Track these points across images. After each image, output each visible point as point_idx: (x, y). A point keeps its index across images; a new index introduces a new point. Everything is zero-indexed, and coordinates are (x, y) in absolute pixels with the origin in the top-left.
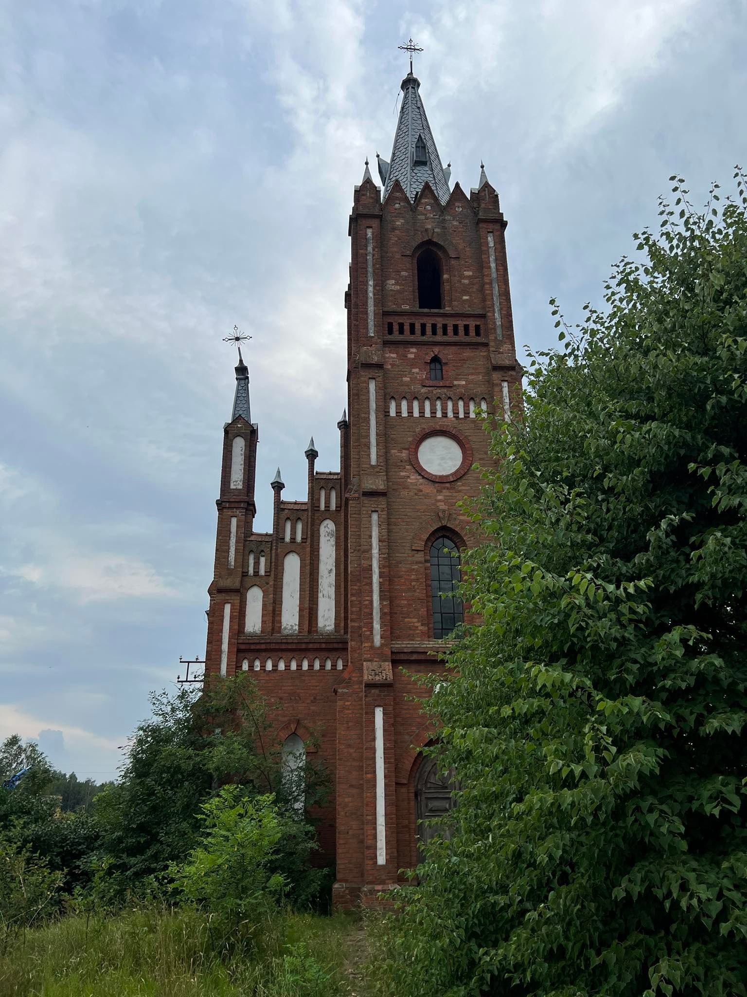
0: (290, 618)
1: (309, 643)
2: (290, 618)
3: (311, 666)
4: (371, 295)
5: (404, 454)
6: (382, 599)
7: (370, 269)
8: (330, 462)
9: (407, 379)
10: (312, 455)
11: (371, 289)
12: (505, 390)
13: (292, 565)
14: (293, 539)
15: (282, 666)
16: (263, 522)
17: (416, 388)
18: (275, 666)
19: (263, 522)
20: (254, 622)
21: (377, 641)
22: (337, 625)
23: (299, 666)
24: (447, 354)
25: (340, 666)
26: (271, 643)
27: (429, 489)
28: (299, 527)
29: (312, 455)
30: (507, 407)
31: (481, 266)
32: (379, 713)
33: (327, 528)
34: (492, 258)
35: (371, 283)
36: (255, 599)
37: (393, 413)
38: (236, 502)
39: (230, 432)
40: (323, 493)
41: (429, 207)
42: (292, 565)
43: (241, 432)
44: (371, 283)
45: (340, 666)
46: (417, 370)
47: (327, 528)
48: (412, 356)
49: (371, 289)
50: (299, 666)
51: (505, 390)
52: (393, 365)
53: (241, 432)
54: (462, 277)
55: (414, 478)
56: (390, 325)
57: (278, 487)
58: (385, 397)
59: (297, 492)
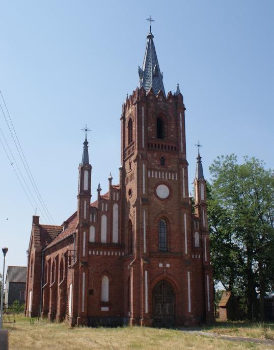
0: (104, 239)
1: (109, 245)
2: (104, 239)
3: (111, 254)
5: (152, 191)
6: (146, 239)
7: (143, 122)
8: (116, 182)
9: (153, 164)
10: (110, 180)
12: (183, 171)
13: (104, 219)
14: (104, 210)
15: (101, 253)
18: (99, 253)
20: (92, 238)
21: (145, 251)
22: (119, 241)
23: (107, 254)
24: (166, 155)
25: (123, 254)
26: (97, 245)
27: (160, 203)
28: (106, 205)
29: (110, 180)
30: (184, 177)
33: (116, 207)
34: (181, 122)
36: (92, 230)
37: (149, 176)
38: (84, 195)
40: (114, 193)
41: (161, 99)
42: (104, 219)
43: (86, 168)
45: (123, 254)
46: (156, 161)
48: (155, 156)
50: (107, 254)
51: (183, 171)
52: (150, 159)
53: (86, 168)
54: (171, 128)
55: (155, 199)
56: (149, 144)
57: (99, 190)
58: (148, 169)
59: (105, 191)
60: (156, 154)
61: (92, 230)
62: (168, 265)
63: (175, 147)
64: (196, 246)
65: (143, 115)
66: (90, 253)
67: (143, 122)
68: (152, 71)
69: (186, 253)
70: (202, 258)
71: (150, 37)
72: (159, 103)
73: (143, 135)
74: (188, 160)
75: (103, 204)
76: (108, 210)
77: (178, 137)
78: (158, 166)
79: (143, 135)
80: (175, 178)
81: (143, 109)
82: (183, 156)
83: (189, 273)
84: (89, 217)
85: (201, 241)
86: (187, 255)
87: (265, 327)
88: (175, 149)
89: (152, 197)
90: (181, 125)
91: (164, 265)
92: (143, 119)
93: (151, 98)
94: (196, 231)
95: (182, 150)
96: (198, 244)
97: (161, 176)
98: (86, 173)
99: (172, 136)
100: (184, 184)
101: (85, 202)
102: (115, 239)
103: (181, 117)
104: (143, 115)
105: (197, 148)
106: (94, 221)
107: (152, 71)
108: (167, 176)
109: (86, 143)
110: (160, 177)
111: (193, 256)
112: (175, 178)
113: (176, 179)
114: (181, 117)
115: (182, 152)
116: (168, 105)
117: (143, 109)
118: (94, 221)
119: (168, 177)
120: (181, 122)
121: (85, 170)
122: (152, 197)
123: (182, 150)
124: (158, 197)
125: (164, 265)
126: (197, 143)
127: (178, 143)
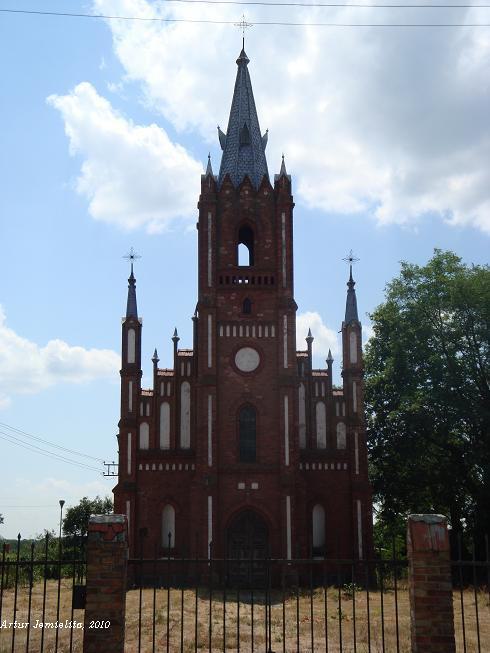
0: (165, 442)
2: (165, 442)
4: (210, 259)
5: (227, 360)
7: (210, 242)
8: (187, 344)
9: (230, 313)
10: (176, 340)
11: (210, 255)
12: (285, 320)
13: (165, 410)
16: (147, 383)
17: (236, 318)
18: (157, 467)
19: (147, 383)
20: (145, 442)
26: (154, 453)
28: (169, 385)
29: (176, 340)
30: (285, 331)
31: (277, 236)
32: (210, 499)
33: (186, 387)
34: (284, 232)
35: (210, 251)
36: (145, 430)
37: (221, 335)
38: (131, 372)
39: (126, 328)
41: (247, 192)
42: (165, 410)
43: (132, 325)
44: (210, 251)
47: (186, 387)
48: (233, 298)
49: (210, 255)
51: (285, 320)
52: (222, 304)
53: (132, 325)
55: (233, 374)
56: (221, 278)
57: (155, 361)
59: (167, 363)
60: (234, 294)
61: (145, 430)
62: (255, 486)
63: (272, 279)
64: (338, 447)
65: (210, 227)
66: (141, 467)
67: (210, 242)
68: (243, 134)
69: (287, 463)
70: (351, 467)
71: (243, 61)
72: (241, 201)
73: (210, 265)
74: (297, 298)
75: (162, 384)
76: (172, 394)
77: (278, 259)
78: (240, 317)
79: (210, 265)
80: (270, 333)
81: (210, 217)
82: (287, 292)
83: (288, 499)
84: (139, 406)
85: (350, 438)
86: (288, 467)
87: (477, 592)
88: (272, 283)
89: (227, 372)
90: (284, 236)
91: (248, 485)
92: (210, 234)
93: (228, 192)
94: (339, 420)
95: (285, 282)
96: (344, 443)
97: (244, 333)
98: (132, 334)
99: (267, 258)
100: (285, 343)
101: (131, 384)
102: (185, 442)
103: (284, 221)
104: (210, 227)
105: (347, 265)
106: (148, 414)
107: (243, 134)
108: (255, 332)
109: (132, 281)
110: (241, 335)
111: (193, 468)
112: (270, 333)
113: (273, 335)
114: (284, 221)
115: (285, 285)
116: (259, 201)
117: (210, 217)
118: (148, 414)
119: (257, 334)
120: (284, 232)
121: (129, 329)
122: (227, 372)
123: (285, 282)
124: (237, 370)
125: (248, 485)
126: (347, 255)
127: (278, 273)
